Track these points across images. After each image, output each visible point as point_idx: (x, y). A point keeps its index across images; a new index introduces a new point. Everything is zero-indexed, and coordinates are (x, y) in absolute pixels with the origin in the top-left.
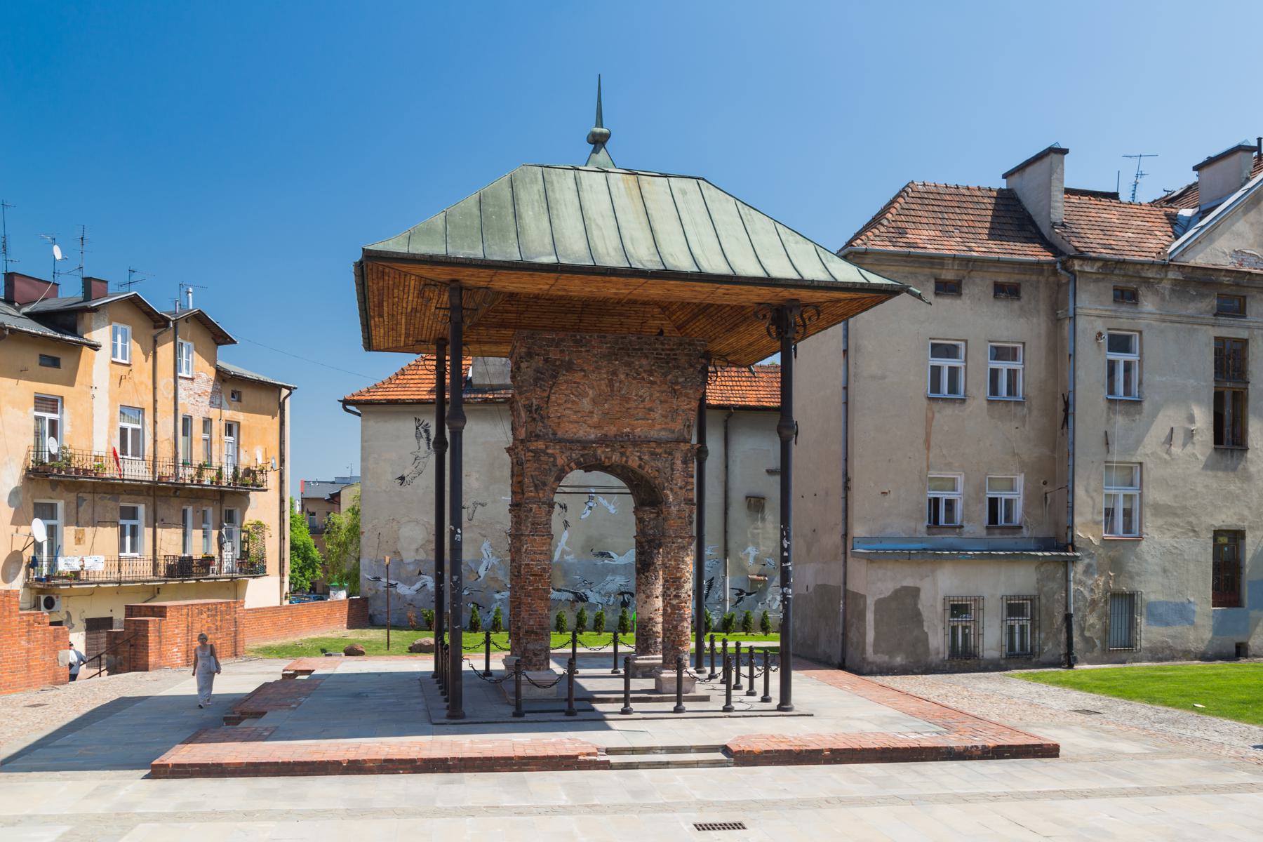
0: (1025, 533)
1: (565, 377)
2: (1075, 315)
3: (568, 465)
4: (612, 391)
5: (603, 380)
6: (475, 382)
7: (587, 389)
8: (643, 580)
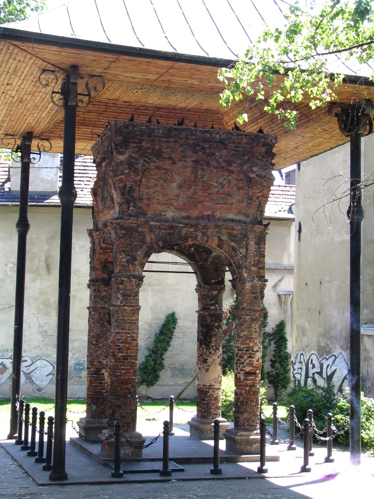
1: (155, 164)
5: (189, 167)
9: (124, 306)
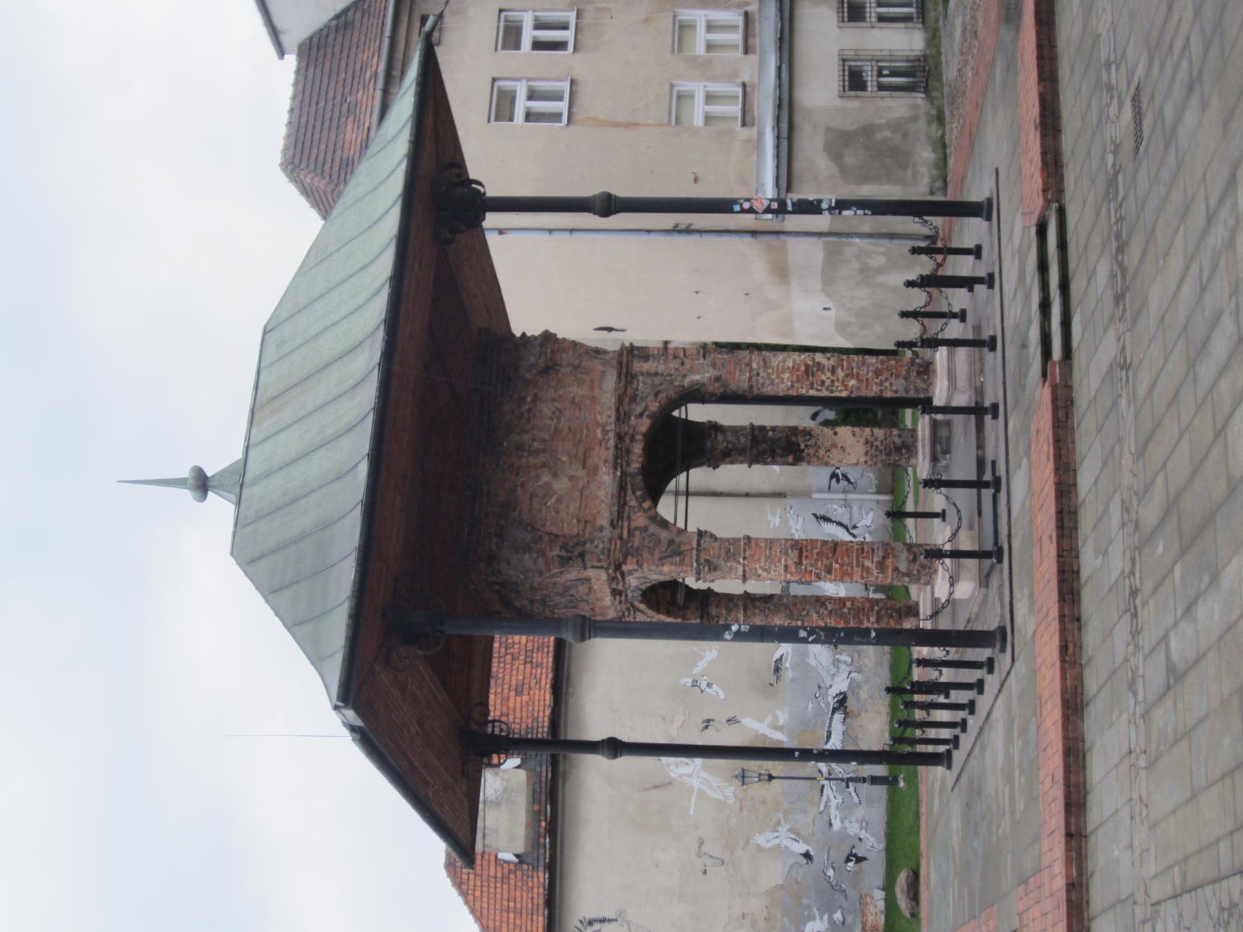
0: (753, 8)
3: (645, 511)
4: (544, 451)
6: (520, 850)
7: (540, 484)
8: (812, 451)
9: (744, 558)
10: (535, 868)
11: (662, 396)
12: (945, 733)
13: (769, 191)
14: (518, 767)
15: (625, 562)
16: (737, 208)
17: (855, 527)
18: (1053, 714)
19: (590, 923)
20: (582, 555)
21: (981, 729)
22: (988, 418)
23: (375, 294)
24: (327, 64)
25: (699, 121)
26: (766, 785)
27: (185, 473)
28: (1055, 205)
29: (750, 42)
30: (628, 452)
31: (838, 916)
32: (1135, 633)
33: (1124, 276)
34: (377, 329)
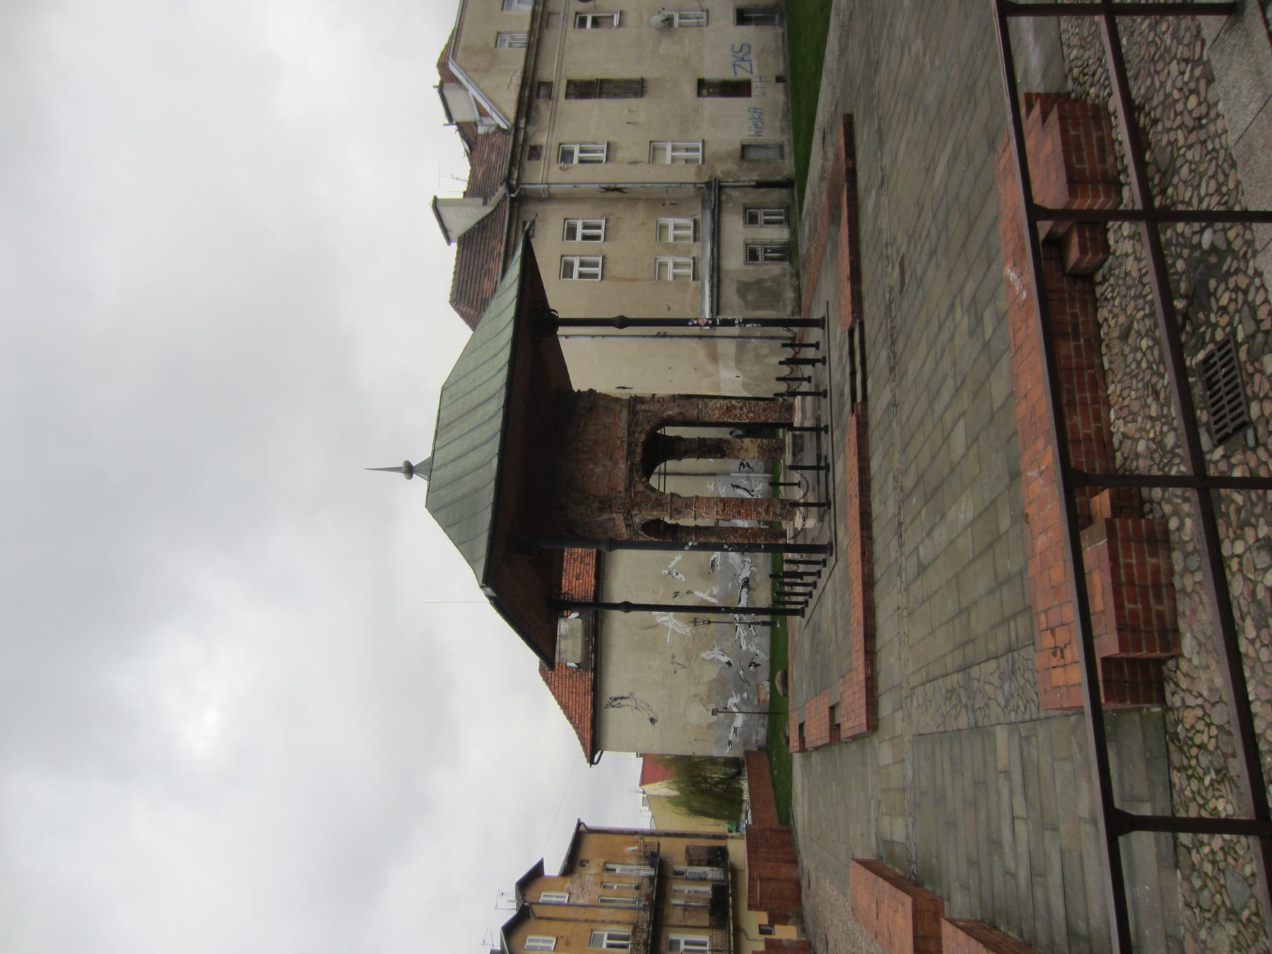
0: (698, 217)
2: (547, 184)
3: (643, 483)
8: (730, 451)
10: (587, 670)
11: (652, 423)
12: (801, 599)
13: (707, 315)
14: (577, 617)
15: (633, 509)
16: (690, 323)
17: (753, 491)
18: (858, 589)
19: (616, 699)
20: (610, 506)
21: (820, 596)
22: (823, 433)
23: (501, 370)
24: (474, 248)
25: (670, 278)
26: (707, 626)
27: (401, 465)
28: (858, 321)
29: (697, 235)
30: (634, 452)
31: (745, 695)
32: (901, 546)
33: (895, 358)
34: (502, 388)
